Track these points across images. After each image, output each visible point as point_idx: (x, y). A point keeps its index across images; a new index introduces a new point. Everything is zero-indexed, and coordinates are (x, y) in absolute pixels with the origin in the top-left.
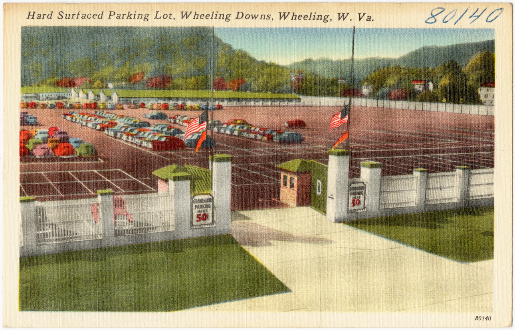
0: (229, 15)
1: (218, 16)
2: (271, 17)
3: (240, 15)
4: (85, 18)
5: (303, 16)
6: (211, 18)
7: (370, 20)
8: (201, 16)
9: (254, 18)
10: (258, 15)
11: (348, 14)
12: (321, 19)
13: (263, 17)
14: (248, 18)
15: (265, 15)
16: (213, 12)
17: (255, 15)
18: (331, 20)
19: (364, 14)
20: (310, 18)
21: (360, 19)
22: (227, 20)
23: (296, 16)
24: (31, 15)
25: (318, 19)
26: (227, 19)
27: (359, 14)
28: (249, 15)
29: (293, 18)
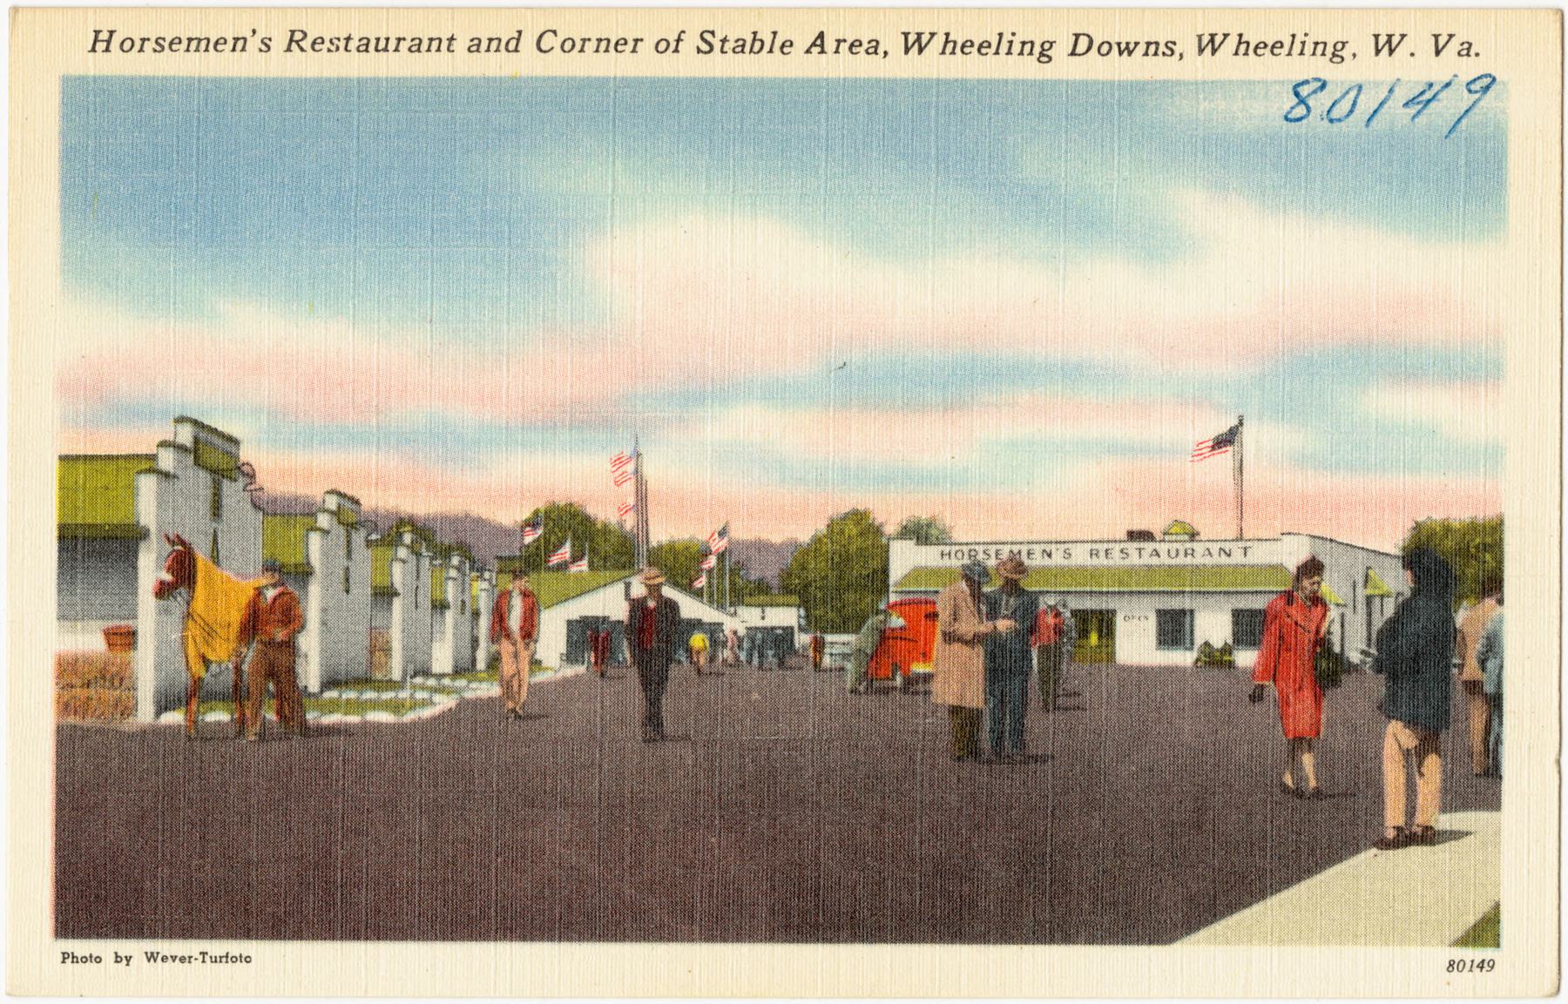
0: (1051, 44)
1: (1016, 48)
2: (1177, 49)
3: (1083, 44)
4: (367, 51)
7: (1468, 55)
8: (617, 44)
9: (1126, 52)
10: (1137, 44)
11: (1403, 36)
12: (1323, 54)
13: (1152, 48)
14: (1108, 53)
17: (1128, 44)
18: (1354, 55)
19: (1451, 36)
21: (1438, 53)
24: (102, 41)
25: (488, 50)
26: (1045, 56)
27: (1436, 37)
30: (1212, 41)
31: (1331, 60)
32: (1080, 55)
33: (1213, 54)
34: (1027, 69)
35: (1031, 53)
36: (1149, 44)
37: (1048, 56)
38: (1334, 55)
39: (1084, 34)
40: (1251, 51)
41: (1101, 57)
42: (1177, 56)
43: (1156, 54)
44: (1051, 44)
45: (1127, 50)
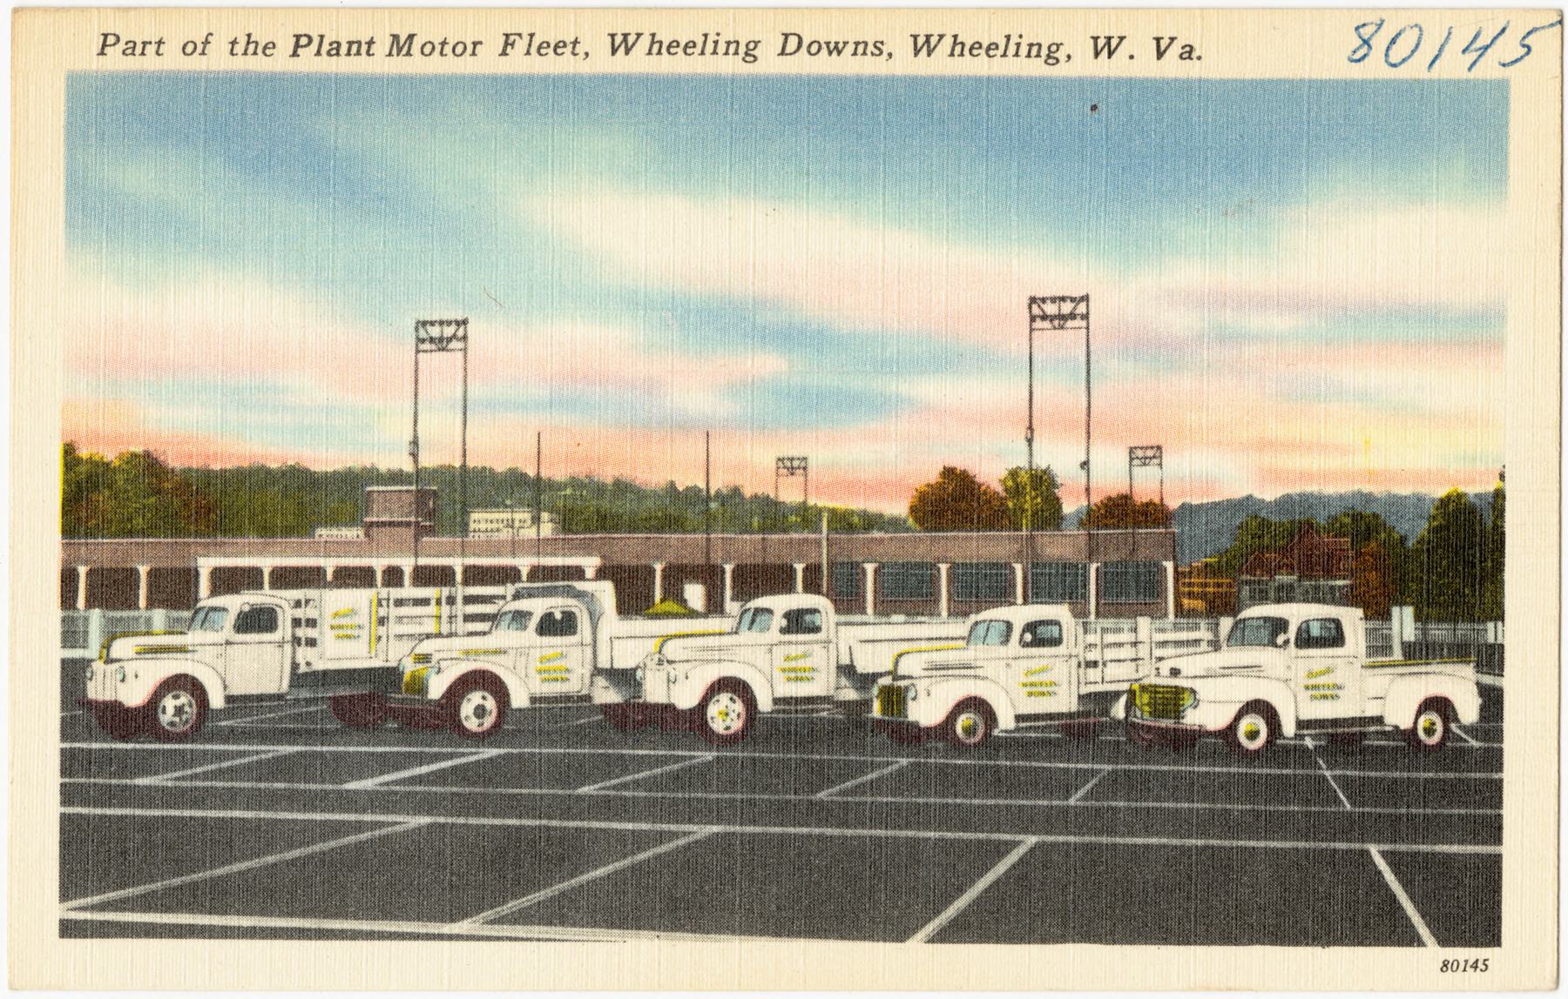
2: (885, 49)
5: (985, 45)
6: (700, 52)
10: (845, 43)
11: (1122, 38)
15: (866, 44)
16: (706, 36)
17: (837, 43)
18: (1069, 57)
19: (1172, 39)
20: (1006, 50)
21: (1160, 55)
22: (748, 59)
23: (963, 44)
26: (750, 55)
28: (819, 42)
29: (953, 50)
30: (928, 41)
31: (1046, 62)
32: (791, 54)
33: (929, 55)
34: (730, 66)
35: (736, 53)
36: (857, 44)
37: (754, 56)
38: (1049, 56)
39: (795, 34)
40: (966, 51)
41: (808, 56)
42: (885, 55)
43: (864, 53)
44: (756, 43)
45: (836, 49)
